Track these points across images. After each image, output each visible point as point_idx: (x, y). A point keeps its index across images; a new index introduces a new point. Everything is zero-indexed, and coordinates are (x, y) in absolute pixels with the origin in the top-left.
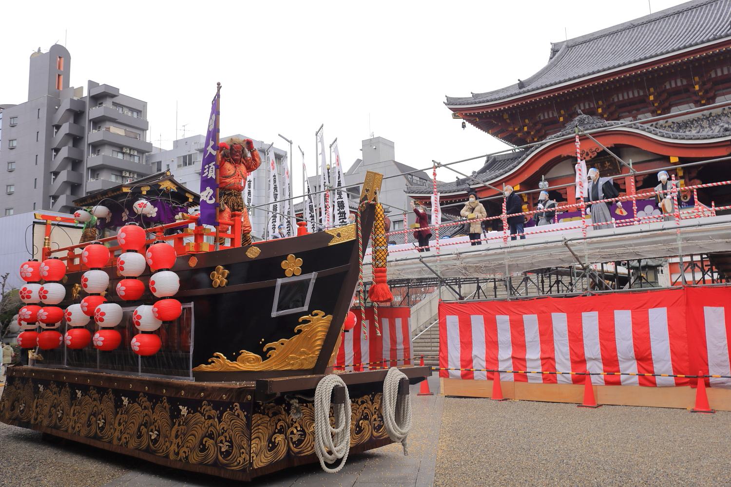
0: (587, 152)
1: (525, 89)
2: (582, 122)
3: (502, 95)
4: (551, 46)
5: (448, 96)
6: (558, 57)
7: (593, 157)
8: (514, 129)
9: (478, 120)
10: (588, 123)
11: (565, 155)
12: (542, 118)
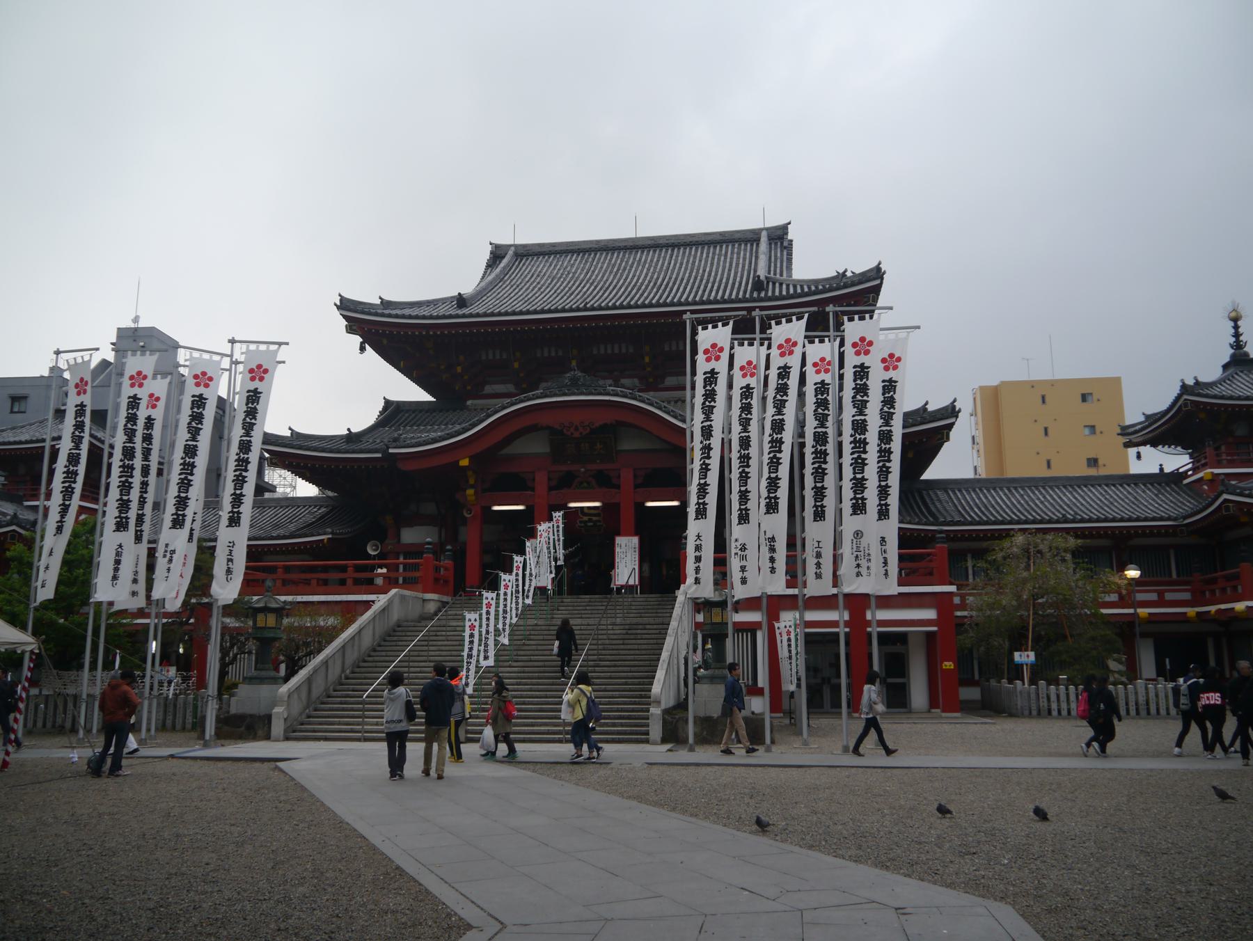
1: (466, 311)
2: (574, 381)
3: (425, 311)
4: (489, 248)
6: (504, 268)
9: (385, 342)
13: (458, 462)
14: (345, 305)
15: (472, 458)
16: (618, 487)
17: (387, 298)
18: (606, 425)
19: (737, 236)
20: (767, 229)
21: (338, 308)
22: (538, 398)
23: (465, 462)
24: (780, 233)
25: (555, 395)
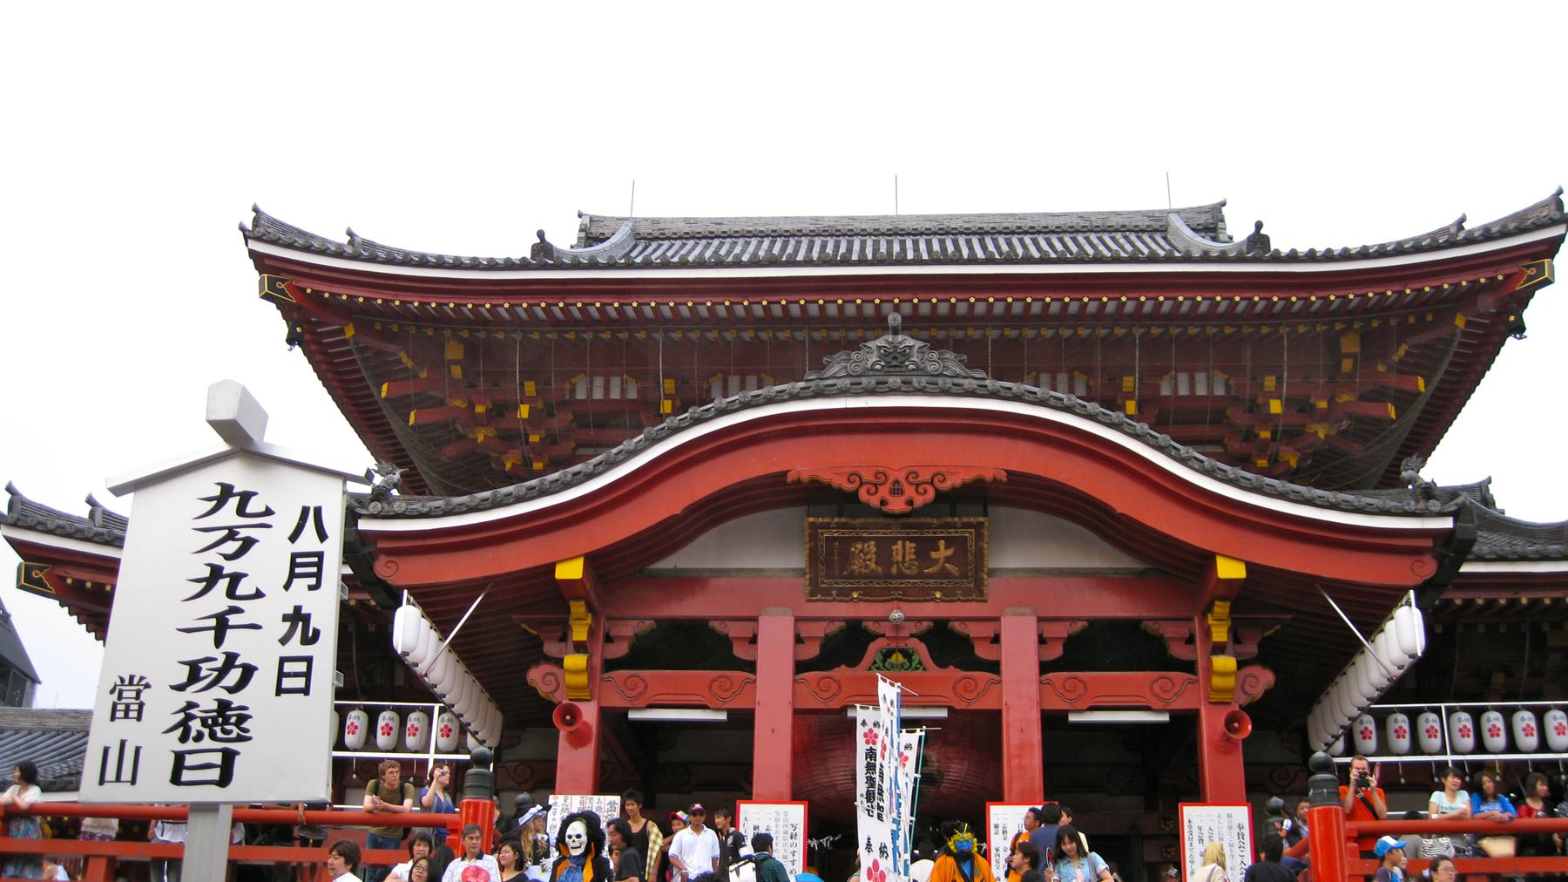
0: (897, 482)
2: (895, 360)
5: (262, 208)
7: (919, 501)
8: (472, 406)
9: (350, 332)
10: (919, 371)
11: (805, 478)
12: (581, 395)
13: (551, 568)
14: (261, 230)
15: (592, 560)
16: (994, 667)
17: (363, 234)
18: (979, 482)
19: (1114, 221)
20: (1178, 212)
21: (247, 236)
22: (795, 397)
23: (570, 570)
24: (1203, 219)
25: (843, 393)
